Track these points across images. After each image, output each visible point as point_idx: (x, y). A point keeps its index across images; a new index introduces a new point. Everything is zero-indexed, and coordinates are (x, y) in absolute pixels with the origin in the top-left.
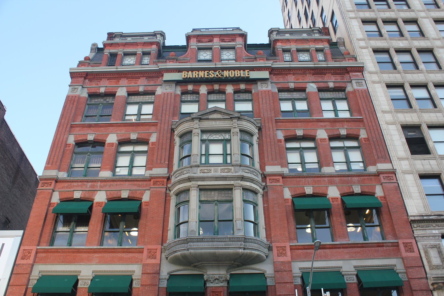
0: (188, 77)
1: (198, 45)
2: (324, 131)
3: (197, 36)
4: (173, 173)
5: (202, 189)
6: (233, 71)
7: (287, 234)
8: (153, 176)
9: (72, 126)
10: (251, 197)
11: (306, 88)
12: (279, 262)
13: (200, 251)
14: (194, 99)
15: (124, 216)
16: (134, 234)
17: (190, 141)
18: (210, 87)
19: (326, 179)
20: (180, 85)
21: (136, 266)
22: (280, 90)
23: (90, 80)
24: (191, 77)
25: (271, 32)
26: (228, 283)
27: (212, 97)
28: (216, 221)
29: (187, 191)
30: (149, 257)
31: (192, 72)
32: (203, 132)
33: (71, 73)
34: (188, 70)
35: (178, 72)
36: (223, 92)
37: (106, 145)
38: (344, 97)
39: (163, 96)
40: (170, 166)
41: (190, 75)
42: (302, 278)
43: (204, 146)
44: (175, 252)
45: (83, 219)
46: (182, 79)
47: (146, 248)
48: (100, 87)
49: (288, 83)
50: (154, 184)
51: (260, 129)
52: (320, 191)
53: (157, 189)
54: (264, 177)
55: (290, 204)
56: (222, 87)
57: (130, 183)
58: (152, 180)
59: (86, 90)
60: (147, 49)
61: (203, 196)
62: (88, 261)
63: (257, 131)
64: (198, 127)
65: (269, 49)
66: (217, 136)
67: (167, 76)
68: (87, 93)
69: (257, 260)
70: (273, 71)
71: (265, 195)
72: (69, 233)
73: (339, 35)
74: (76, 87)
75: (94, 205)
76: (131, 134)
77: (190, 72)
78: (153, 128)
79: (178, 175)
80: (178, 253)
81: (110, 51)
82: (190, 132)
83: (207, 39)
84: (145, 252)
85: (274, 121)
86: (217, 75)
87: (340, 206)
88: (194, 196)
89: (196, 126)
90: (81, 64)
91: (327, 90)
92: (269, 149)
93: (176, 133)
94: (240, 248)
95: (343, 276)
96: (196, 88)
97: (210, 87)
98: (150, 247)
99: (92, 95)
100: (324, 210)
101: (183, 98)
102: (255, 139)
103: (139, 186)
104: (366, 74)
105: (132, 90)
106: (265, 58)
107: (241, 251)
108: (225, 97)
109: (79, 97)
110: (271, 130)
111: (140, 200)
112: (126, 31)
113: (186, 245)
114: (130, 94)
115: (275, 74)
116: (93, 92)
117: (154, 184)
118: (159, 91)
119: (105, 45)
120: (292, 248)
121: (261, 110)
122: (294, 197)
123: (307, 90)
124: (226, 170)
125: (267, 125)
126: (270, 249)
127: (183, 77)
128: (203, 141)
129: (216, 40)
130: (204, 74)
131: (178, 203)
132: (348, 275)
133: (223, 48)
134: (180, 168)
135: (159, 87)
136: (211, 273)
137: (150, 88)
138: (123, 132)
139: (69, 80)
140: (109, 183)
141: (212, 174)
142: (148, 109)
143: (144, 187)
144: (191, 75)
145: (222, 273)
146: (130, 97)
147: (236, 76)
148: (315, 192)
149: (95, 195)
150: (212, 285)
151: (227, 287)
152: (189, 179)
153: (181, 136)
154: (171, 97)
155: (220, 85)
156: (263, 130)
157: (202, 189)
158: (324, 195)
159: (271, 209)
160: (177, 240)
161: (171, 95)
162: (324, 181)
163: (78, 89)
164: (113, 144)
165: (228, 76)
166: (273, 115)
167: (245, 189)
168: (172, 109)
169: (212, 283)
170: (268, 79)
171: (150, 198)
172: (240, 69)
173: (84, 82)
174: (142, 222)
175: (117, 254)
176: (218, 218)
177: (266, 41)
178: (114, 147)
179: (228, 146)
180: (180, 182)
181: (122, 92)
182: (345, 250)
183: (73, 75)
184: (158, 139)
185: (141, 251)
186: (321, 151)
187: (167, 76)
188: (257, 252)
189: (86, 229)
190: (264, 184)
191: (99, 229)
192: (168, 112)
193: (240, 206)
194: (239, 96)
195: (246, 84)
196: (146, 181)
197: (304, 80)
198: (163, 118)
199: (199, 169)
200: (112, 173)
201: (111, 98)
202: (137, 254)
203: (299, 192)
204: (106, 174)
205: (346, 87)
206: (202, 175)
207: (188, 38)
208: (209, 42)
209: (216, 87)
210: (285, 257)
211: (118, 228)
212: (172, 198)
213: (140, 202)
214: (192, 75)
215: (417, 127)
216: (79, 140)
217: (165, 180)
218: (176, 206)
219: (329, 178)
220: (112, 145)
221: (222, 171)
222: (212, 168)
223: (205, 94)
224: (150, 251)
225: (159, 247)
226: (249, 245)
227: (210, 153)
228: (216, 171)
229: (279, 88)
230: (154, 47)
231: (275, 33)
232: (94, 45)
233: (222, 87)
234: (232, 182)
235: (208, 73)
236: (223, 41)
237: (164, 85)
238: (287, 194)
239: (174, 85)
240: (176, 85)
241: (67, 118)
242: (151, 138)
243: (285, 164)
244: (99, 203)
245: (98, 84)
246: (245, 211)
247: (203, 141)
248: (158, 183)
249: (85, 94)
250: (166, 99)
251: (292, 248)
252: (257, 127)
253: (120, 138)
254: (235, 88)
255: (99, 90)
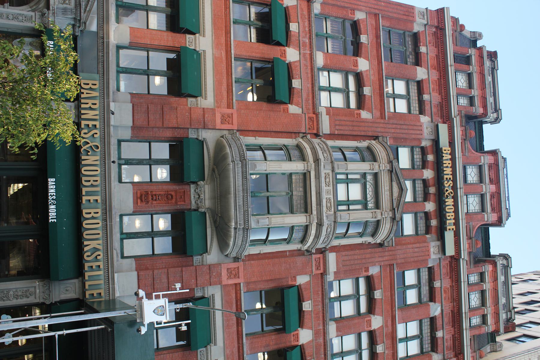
0: (444, 155)
1: (486, 166)
2: (381, 325)
3: (497, 164)
4: (324, 140)
5: (305, 176)
6: (453, 210)
7: (253, 279)
8: (320, 116)
9: (376, 15)
10: (297, 235)
11: (435, 302)
12: (221, 270)
13: (232, 175)
14: (415, 163)
15: (271, 83)
16: (250, 97)
17: (363, 160)
18: (431, 182)
19: (321, 327)
20: (432, 145)
21: (213, 101)
22: (430, 269)
23: (435, 34)
24: (444, 158)
25: (506, 257)
26: (195, 210)
27: (419, 185)
28: (268, 194)
29: (303, 158)
30: (223, 116)
31: (450, 159)
32: (376, 176)
33: (443, 9)
34: (453, 154)
35: (449, 142)
36: (426, 198)
37: (355, 58)
38: (424, 350)
39: (418, 124)
40: (332, 136)
41: (447, 157)
42: (203, 298)
43: (358, 177)
44: (230, 147)
45: (265, 36)
46: (441, 147)
47: (234, 111)
48: (427, 46)
49: (441, 279)
50: (310, 118)
51: (381, 245)
53: (303, 123)
54: (322, 251)
55: (290, 283)
56: (432, 197)
57: (310, 89)
58: (314, 116)
59: (422, 29)
60: (477, 101)
61: (298, 177)
62: (216, 45)
63: (379, 241)
64: (381, 168)
65: (483, 255)
66: (371, 193)
67: (443, 129)
68: (419, 31)
69: (223, 245)
70: (455, 260)
71: (299, 253)
72: (248, 20)
73: (506, 344)
74: (426, 17)
75: (282, 48)
76: (370, 88)
77: (450, 157)
78: (378, 114)
79: (322, 146)
80: (228, 150)
81: (473, 56)
82: (375, 160)
83: (493, 176)
84: (229, 111)
85: (392, 262)
86: (447, 190)
87: (288, 344)
88: (297, 167)
89: (382, 166)
90: (455, 21)
92: (356, 257)
93: (373, 142)
94: (236, 223)
95: (206, 347)
96: (430, 165)
97: (431, 182)
98: (235, 116)
99: (416, 37)
100: (284, 324)
101: (417, 149)
102: (369, 239)
103: (307, 100)
105: (425, 86)
106: (471, 251)
107: (233, 224)
108: (419, 202)
109: (413, 21)
110: (381, 259)
111: (290, 102)
112: (501, 74)
113: (238, 159)
114: (419, 83)
115: (450, 263)
116: (420, 39)
117: (310, 118)
118: (425, 119)
119: (481, 49)
120: (237, 286)
121: (405, 247)
122: (299, 287)
123: (431, 304)
124: (329, 205)
125: (387, 253)
126: (236, 259)
127: (443, 149)
128: (364, 175)
129: (493, 188)
130: (448, 174)
131: (288, 147)
132: (207, 353)
133: (482, 197)
134: (330, 148)
135: (430, 119)
136: (206, 190)
137: (427, 108)
138: (372, 77)
139: (434, 8)
140: (309, 64)
141: (324, 188)
142: (401, 106)
143: (306, 106)
144: (446, 158)
145: (207, 203)
146: (416, 84)
147: (447, 214)
148: (306, 314)
149: (294, 48)
150: (192, 191)
151: (190, 209)
152: (317, 160)
153: (369, 148)
154: (418, 134)
155: (435, 194)
156: (380, 249)
157: (305, 176)
158: (301, 325)
159: (283, 260)
160: (244, 148)
161: (420, 134)
162: (319, 324)
163: (423, 19)
164: (357, 66)
165: (447, 204)
166: (399, 261)
167: (306, 228)
168: (403, 136)
169: (195, 191)
170: (445, 254)
171: (293, 114)
172: (457, 218)
173: (432, 26)
174: (265, 105)
175: (225, 78)
176: (272, 196)
177: (494, 251)
178: (353, 68)
179: (359, 207)
180: (313, 149)
181: (421, 73)
182: (235, 350)
183: (441, 12)
184: (365, 121)
185: (230, 105)
186: (356, 321)
187: (443, 129)
188: (231, 243)
189: (254, 39)
190: (314, 251)
191: (254, 54)
192: (398, 131)
193: (286, 222)
194: (421, 218)
195: (437, 227)
196: (313, 108)
197: (445, 299)
198: (390, 126)
199: (330, 172)
200: (322, 66)
201: (414, 61)
202: (226, 101)
203: (305, 294)
204: (320, 59)
205: (437, 353)
206: (323, 175)
207: (494, 153)
208: (490, 178)
209: (432, 190)
210: (226, 277)
211: (256, 78)
212: (294, 140)
213: (287, 102)
214: (447, 160)
216: (360, 26)
217: (315, 132)
218: (284, 145)
219: (322, 331)
220: (356, 64)
221: (328, 200)
222: (331, 188)
223: (423, 176)
224: (231, 116)
225: (235, 127)
226: (240, 233)
227: (349, 185)
228: (328, 192)
229: (434, 269)
230: (481, 111)
231: (505, 262)
232: (480, 36)
233: (432, 197)
234: (314, 212)
235: (450, 178)
236: (492, 196)
237: (432, 125)
238: (302, 280)
239: (433, 137)
240: (433, 140)
241: (386, 9)
242: (365, 112)
243: (339, 277)
244: (285, 54)
245: (430, 43)
246: (280, 228)
247: (364, 175)
248: (311, 123)
249: (417, 28)
250: (415, 128)
251: (237, 285)
252: (384, 241)
253: (364, 75)
254: (432, 214)
255: (423, 46)
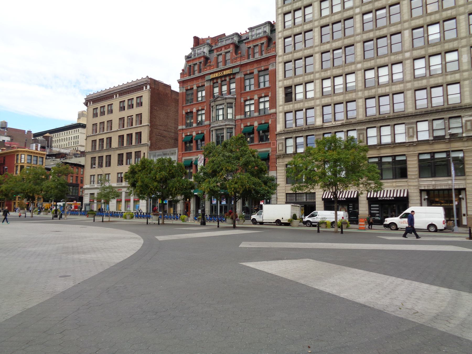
52: (252, 124)
59: (184, 88)
67: (207, 78)
70: (241, 66)
71: (235, 128)
91: (262, 71)
99: (187, 90)
104: (277, 58)
137: (203, 84)
139: (178, 84)
187: (207, 78)
215: (290, 87)
232: (186, 56)
